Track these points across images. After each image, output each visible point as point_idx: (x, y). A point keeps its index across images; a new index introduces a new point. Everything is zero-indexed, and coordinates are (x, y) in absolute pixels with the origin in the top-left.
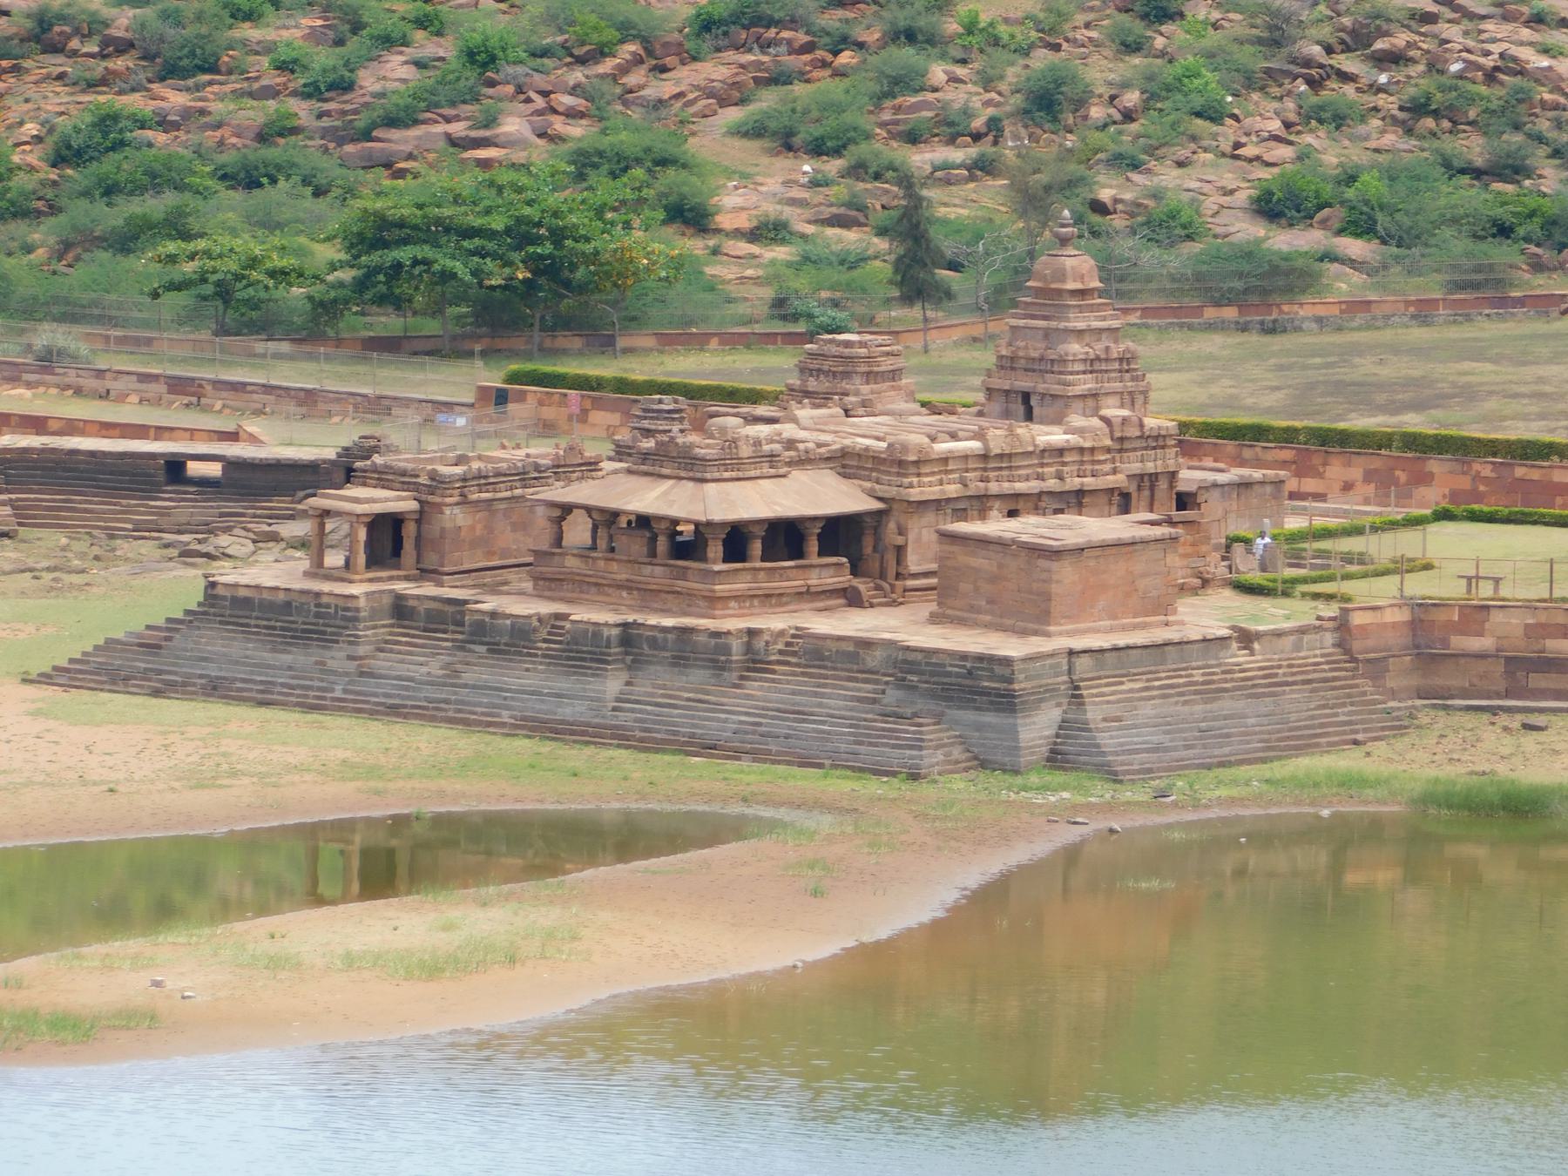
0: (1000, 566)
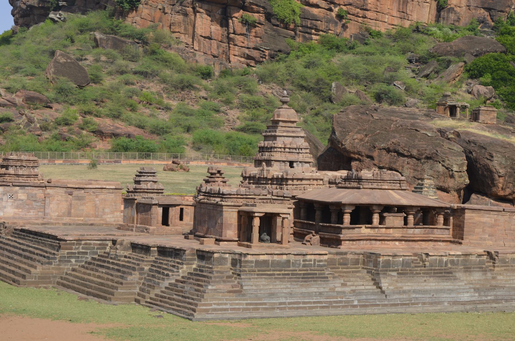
0: (496, 220)
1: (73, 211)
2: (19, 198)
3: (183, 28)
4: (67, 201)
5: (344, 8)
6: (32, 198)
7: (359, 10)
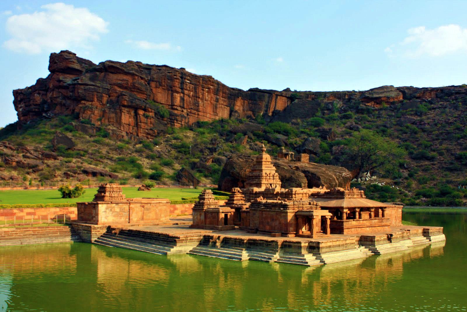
1: (145, 217)
2: (115, 210)
3: (115, 119)
4: (141, 211)
5: (189, 110)
6: (122, 210)
7: (195, 111)
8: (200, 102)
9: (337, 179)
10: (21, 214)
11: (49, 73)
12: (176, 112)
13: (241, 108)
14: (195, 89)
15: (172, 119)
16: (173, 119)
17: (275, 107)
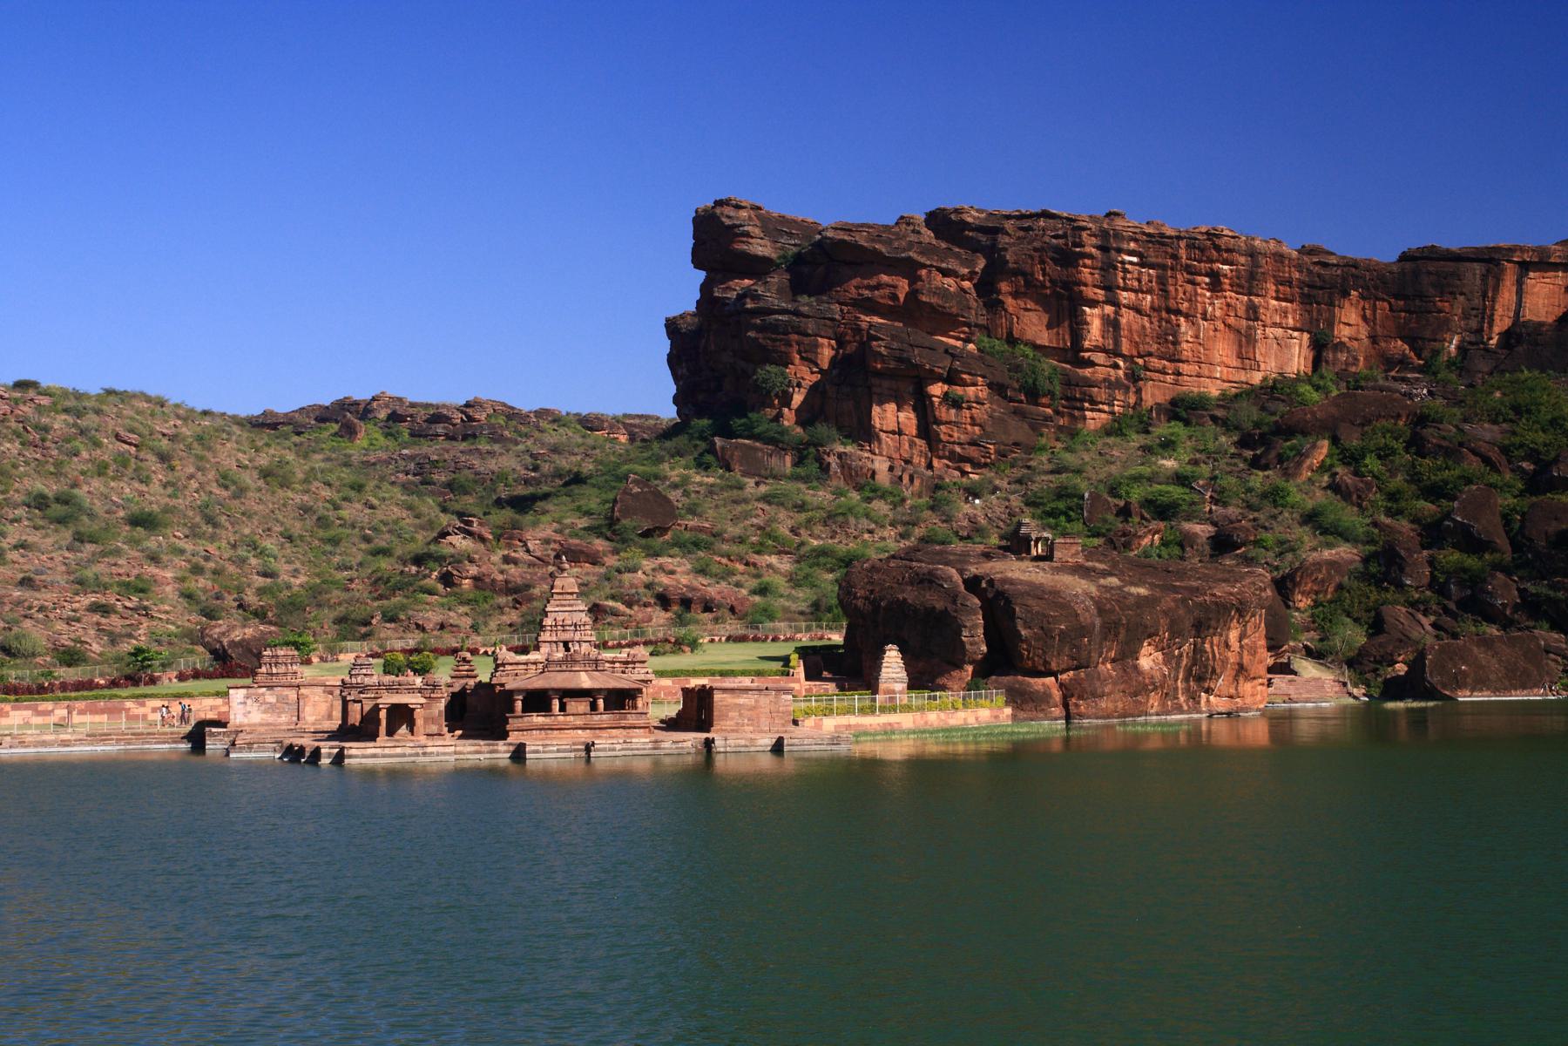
5: (1140, 361)
6: (282, 700)
8: (1183, 329)
9: (1101, 611)
10: (141, 711)
11: (701, 275)
12: (1087, 372)
13: (1363, 332)
14: (1162, 282)
15: (1076, 399)
16: (1076, 397)
17: (1517, 313)
